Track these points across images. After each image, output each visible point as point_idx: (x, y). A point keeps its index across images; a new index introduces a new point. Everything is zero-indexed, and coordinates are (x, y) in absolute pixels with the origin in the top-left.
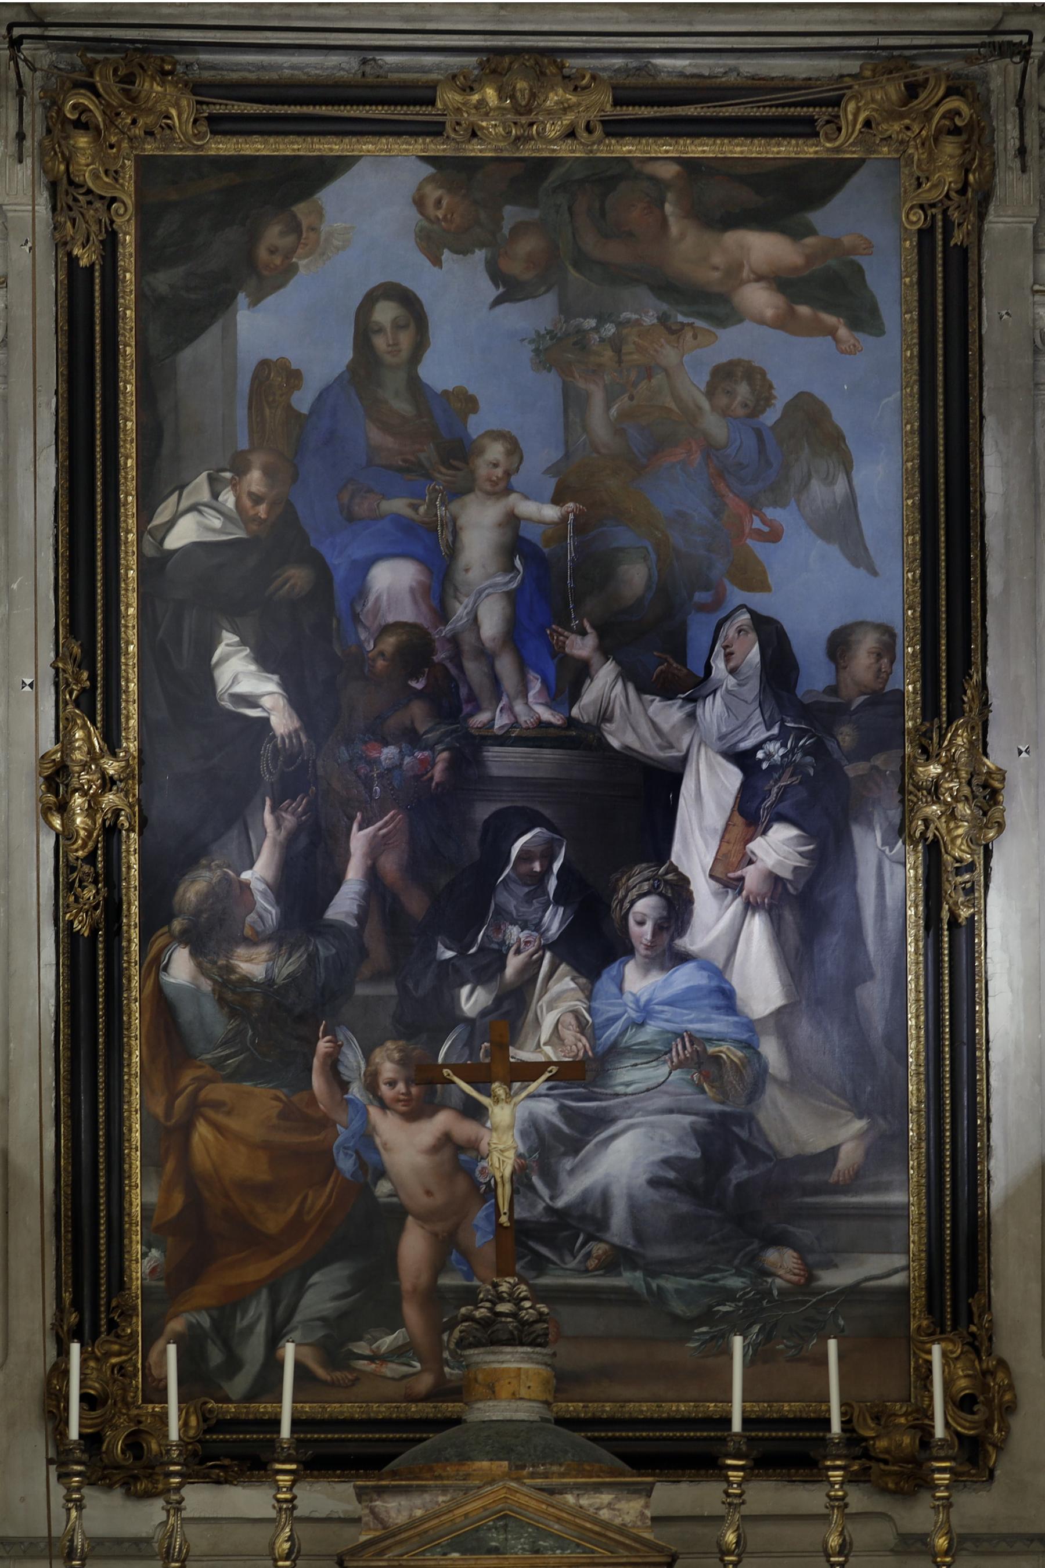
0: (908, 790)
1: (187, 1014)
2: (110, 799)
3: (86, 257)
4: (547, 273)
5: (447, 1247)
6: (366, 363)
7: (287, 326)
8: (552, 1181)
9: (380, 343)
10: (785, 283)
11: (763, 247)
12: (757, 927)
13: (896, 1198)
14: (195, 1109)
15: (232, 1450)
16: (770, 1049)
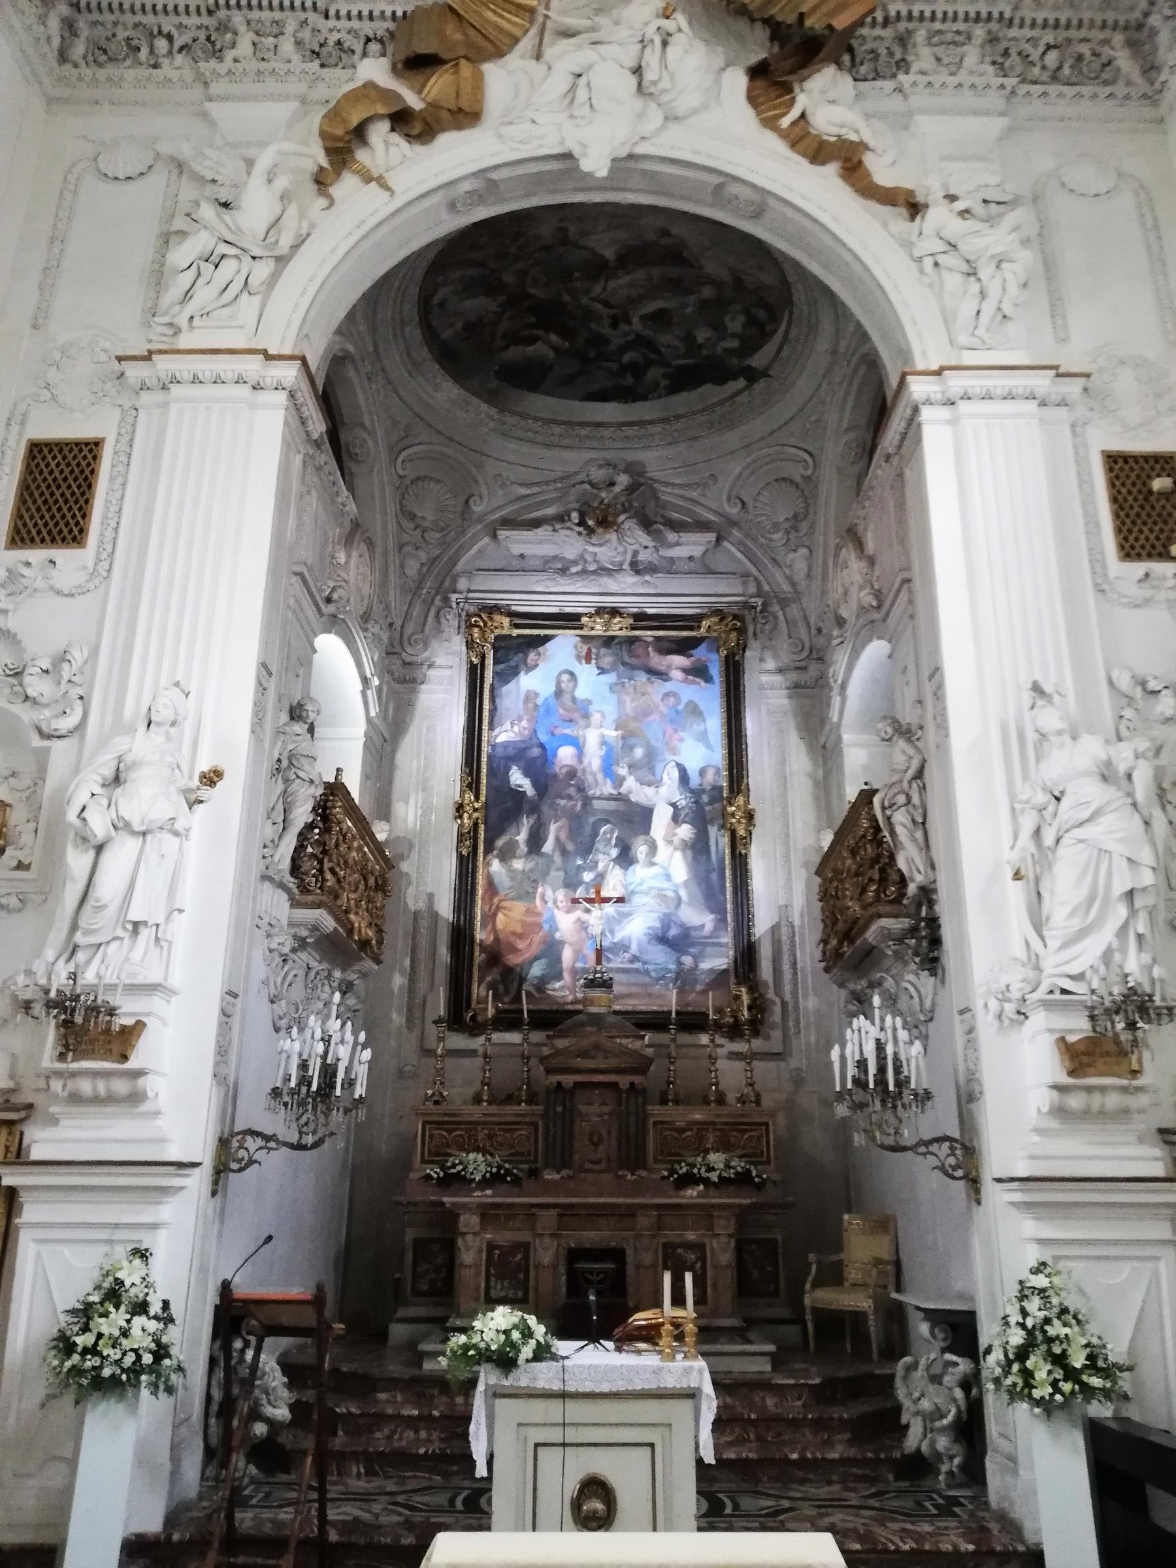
0: (724, 814)
1: (496, 881)
2: (476, 815)
3: (475, 661)
4: (613, 668)
5: (578, 954)
6: (559, 693)
7: (535, 681)
8: (612, 932)
9: (563, 686)
10: (686, 671)
11: (678, 660)
12: (678, 855)
13: (724, 940)
14: (498, 908)
15: (508, 1020)
16: (683, 893)
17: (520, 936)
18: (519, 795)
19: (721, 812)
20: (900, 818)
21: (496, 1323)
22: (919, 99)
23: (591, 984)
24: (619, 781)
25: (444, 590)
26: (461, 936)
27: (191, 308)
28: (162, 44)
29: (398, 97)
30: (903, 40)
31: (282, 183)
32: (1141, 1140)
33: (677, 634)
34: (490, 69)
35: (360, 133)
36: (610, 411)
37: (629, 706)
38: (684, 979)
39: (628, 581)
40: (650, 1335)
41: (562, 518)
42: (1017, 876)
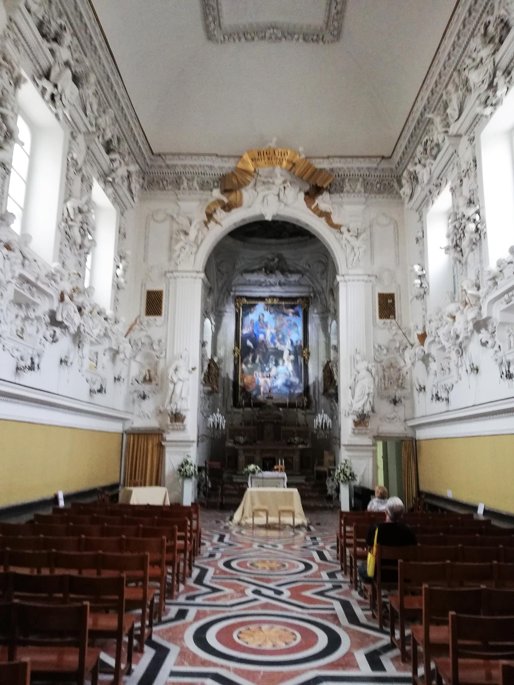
4: (274, 312)
5: (265, 389)
6: (259, 320)
10: (293, 314)
11: (291, 311)
16: (291, 374)
17: (250, 384)
18: (249, 348)
19: (301, 352)
20: (334, 369)
21: (252, 467)
22: (345, 199)
23: (268, 398)
24: (275, 344)
25: (229, 291)
26: (235, 383)
27: (180, 259)
28: (165, 183)
29: (223, 202)
30: (343, 180)
31: (198, 226)
32: (369, 438)
33: (290, 302)
34: (244, 191)
35: (215, 211)
36: (273, 241)
37: (278, 324)
38: (291, 395)
39: (278, 288)
40: (277, 470)
41: (260, 270)
42: (350, 388)
